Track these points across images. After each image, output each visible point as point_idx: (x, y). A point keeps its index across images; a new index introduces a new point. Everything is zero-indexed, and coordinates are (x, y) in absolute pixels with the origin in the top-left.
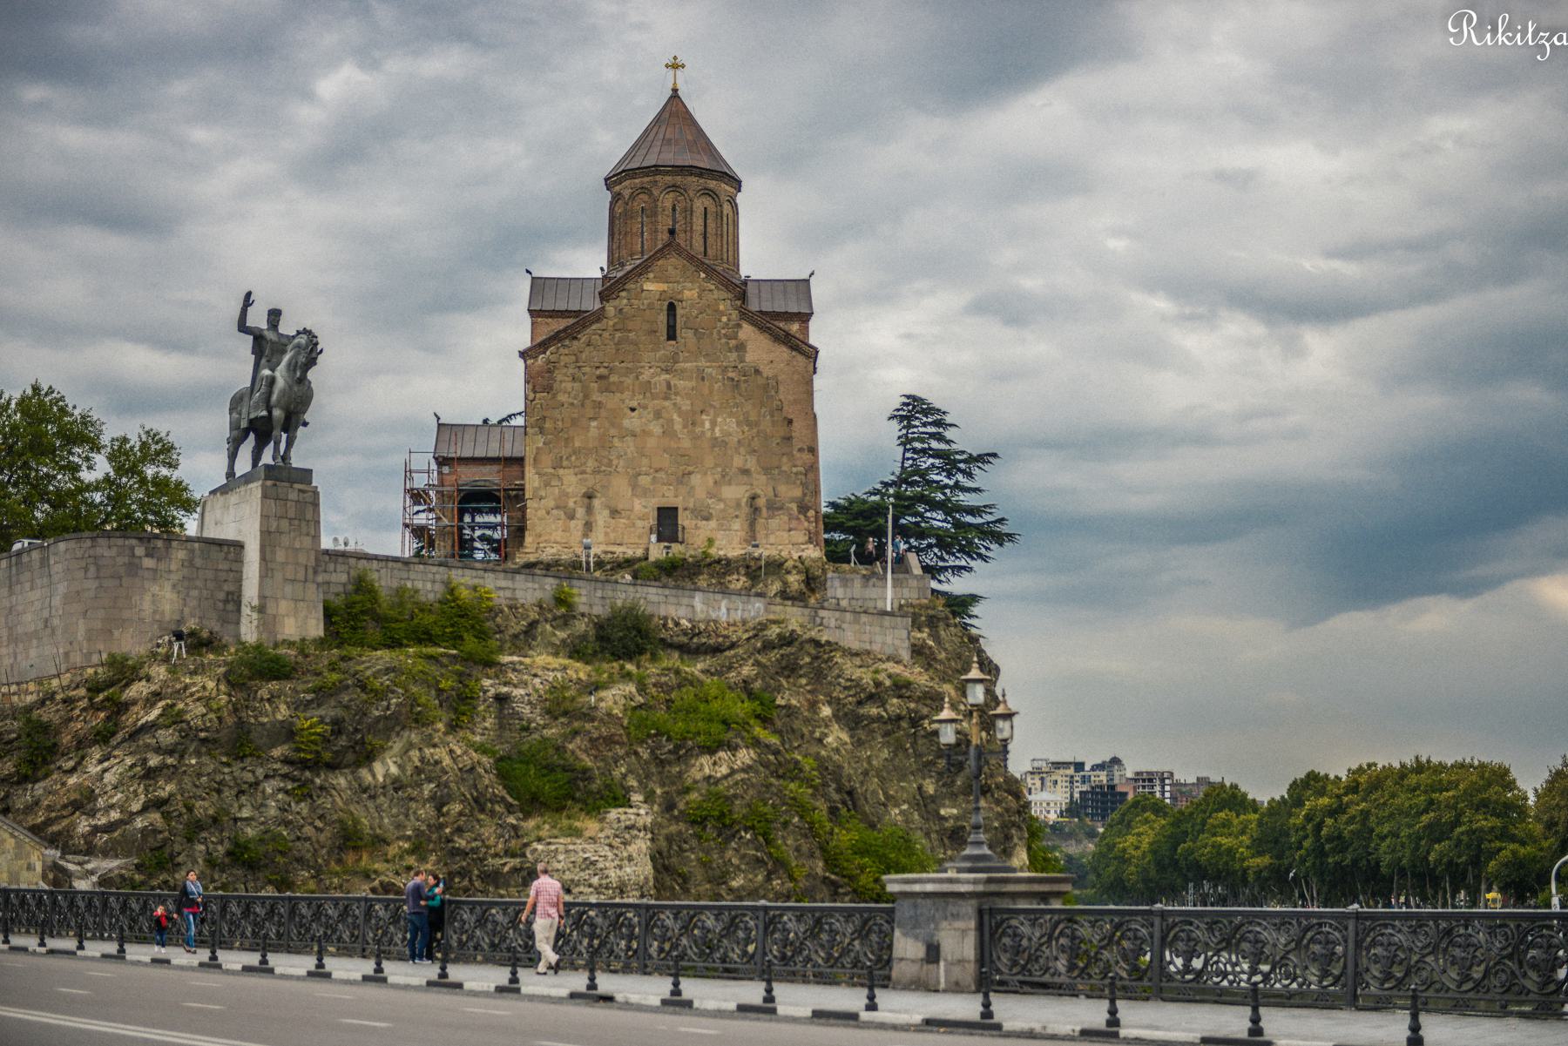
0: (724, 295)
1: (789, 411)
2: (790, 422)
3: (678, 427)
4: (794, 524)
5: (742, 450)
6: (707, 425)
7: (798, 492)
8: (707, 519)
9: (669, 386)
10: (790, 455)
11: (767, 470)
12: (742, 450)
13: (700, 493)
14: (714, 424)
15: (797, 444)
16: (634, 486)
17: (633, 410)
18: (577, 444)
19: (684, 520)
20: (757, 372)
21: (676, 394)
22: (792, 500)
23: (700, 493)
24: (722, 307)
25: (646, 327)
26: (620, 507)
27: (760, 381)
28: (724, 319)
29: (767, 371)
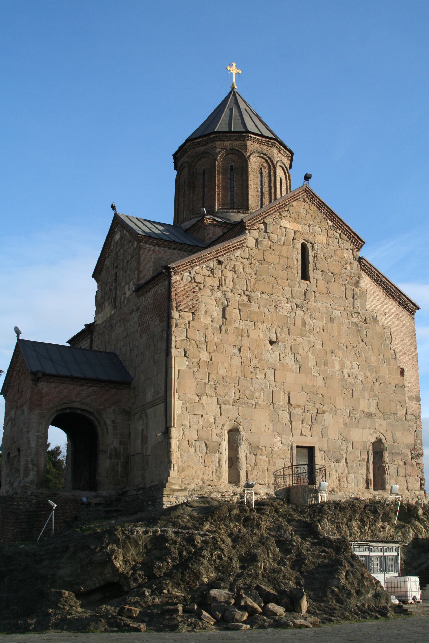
0: (348, 245)
1: (404, 361)
2: (402, 372)
3: (312, 363)
4: (409, 470)
5: (366, 394)
6: (337, 367)
7: (410, 439)
8: (338, 461)
9: (304, 324)
10: (402, 403)
11: (385, 416)
12: (366, 394)
13: (333, 434)
14: (343, 366)
15: (409, 393)
16: (275, 421)
17: (271, 342)
18: (222, 372)
19: (319, 460)
20: (375, 320)
21: (311, 332)
22: (407, 447)
23: (333, 434)
24: (346, 256)
25: (284, 262)
26: (261, 445)
27: (378, 329)
28: (348, 267)
29: (383, 320)
